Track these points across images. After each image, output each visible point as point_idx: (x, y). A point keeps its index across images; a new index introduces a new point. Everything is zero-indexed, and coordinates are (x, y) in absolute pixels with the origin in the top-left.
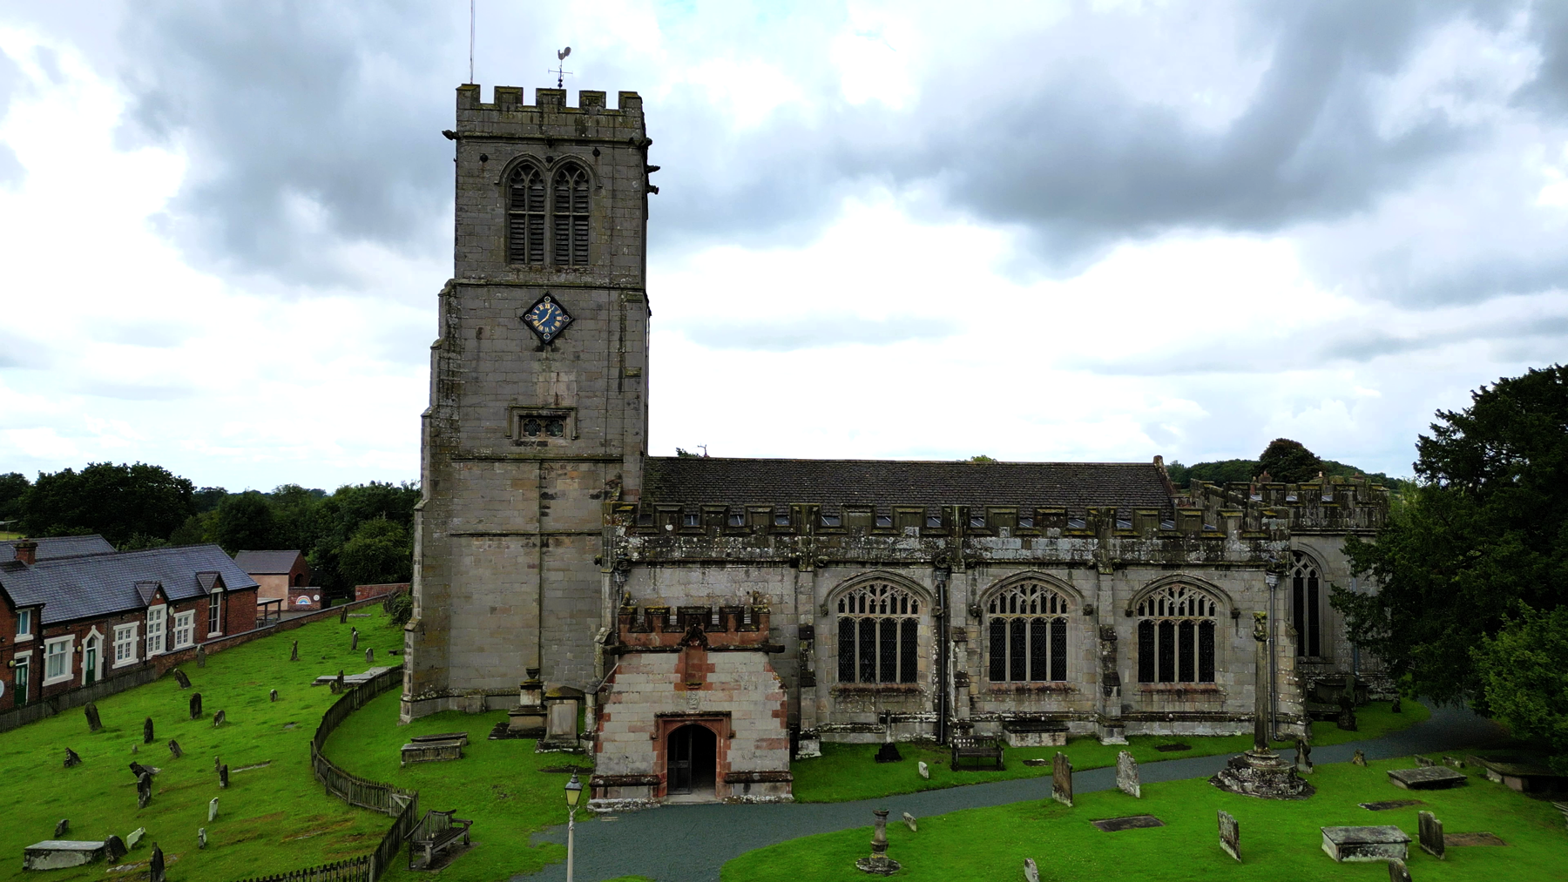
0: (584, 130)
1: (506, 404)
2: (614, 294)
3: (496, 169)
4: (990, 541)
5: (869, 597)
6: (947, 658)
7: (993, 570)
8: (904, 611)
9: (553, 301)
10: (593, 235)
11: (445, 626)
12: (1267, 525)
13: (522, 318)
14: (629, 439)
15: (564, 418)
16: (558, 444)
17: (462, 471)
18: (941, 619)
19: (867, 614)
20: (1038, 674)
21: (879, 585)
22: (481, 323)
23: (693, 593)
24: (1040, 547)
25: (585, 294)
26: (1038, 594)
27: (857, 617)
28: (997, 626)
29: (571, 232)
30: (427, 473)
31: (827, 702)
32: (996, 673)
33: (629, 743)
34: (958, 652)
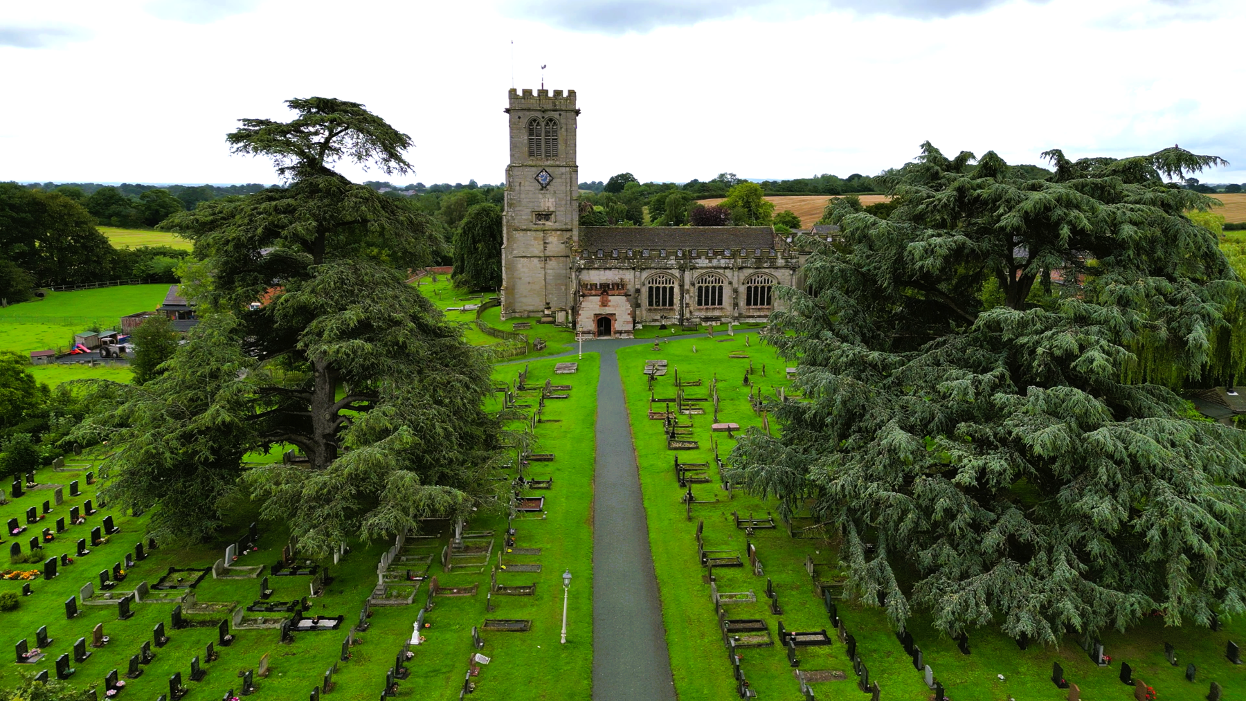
3: (524, 122)
11: (513, 289)
16: (548, 223)
17: (517, 235)
18: (682, 286)
20: (713, 303)
27: (654, 286)
28: (700, 289)
31: (644, 313)
32: (700, 303)
33: (586, 320)
34: (687, 296)
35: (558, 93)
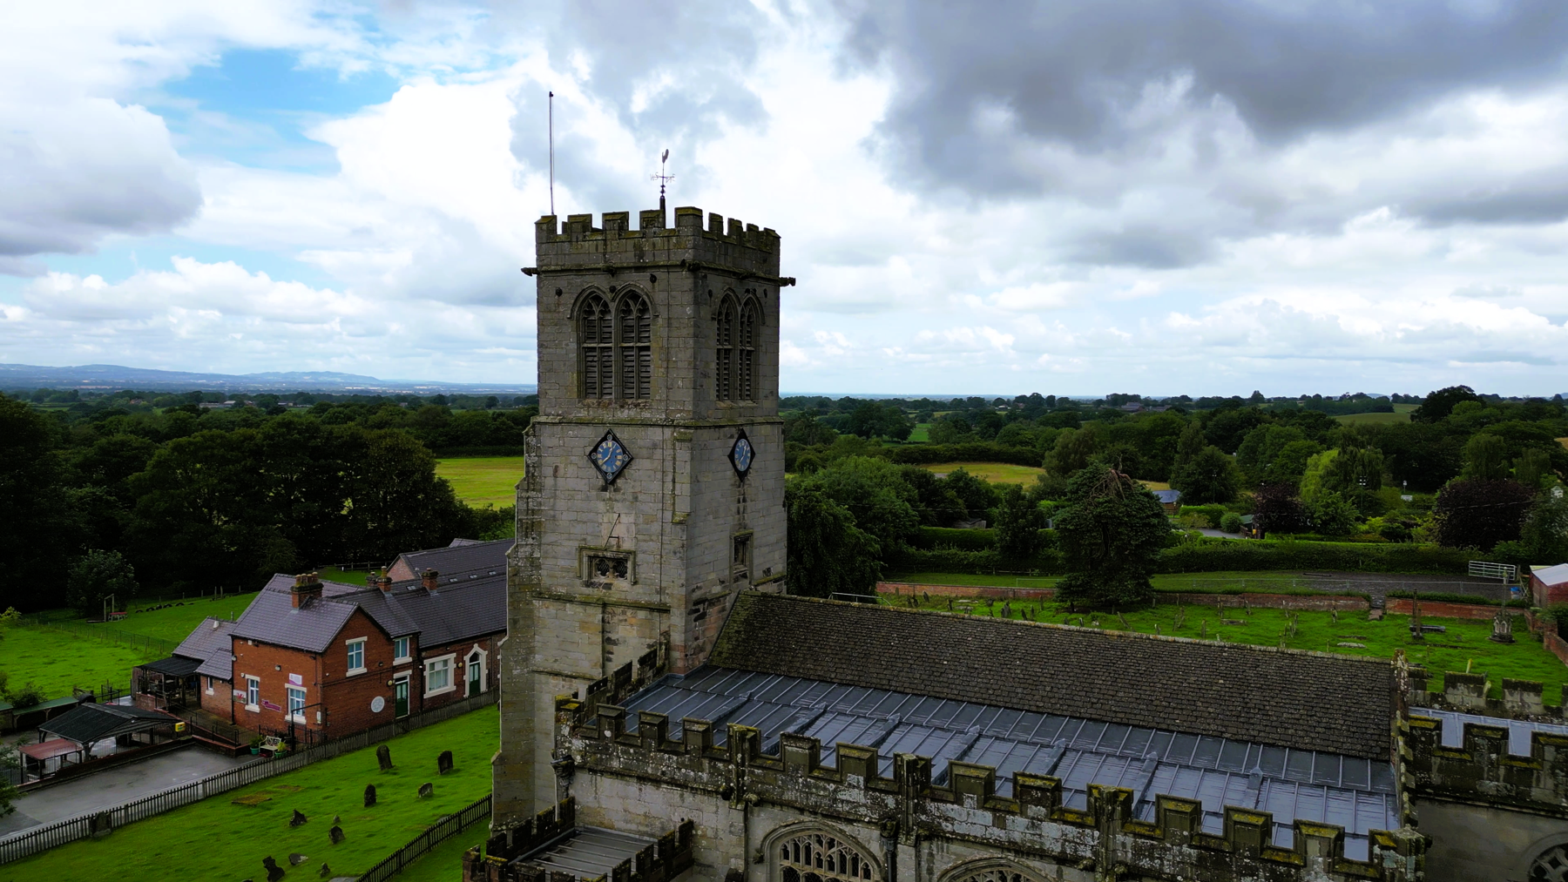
0: (641, 255)
1: (576, 544)
2: (668, 431)
4: (951, 809)
5: (815, 847)
7: (955, 848)
9: (615, 439)
12: (1381, 858)
16: (622, 587)
23: (632, 809)
24: (1018, 828)
25: (641, 432)
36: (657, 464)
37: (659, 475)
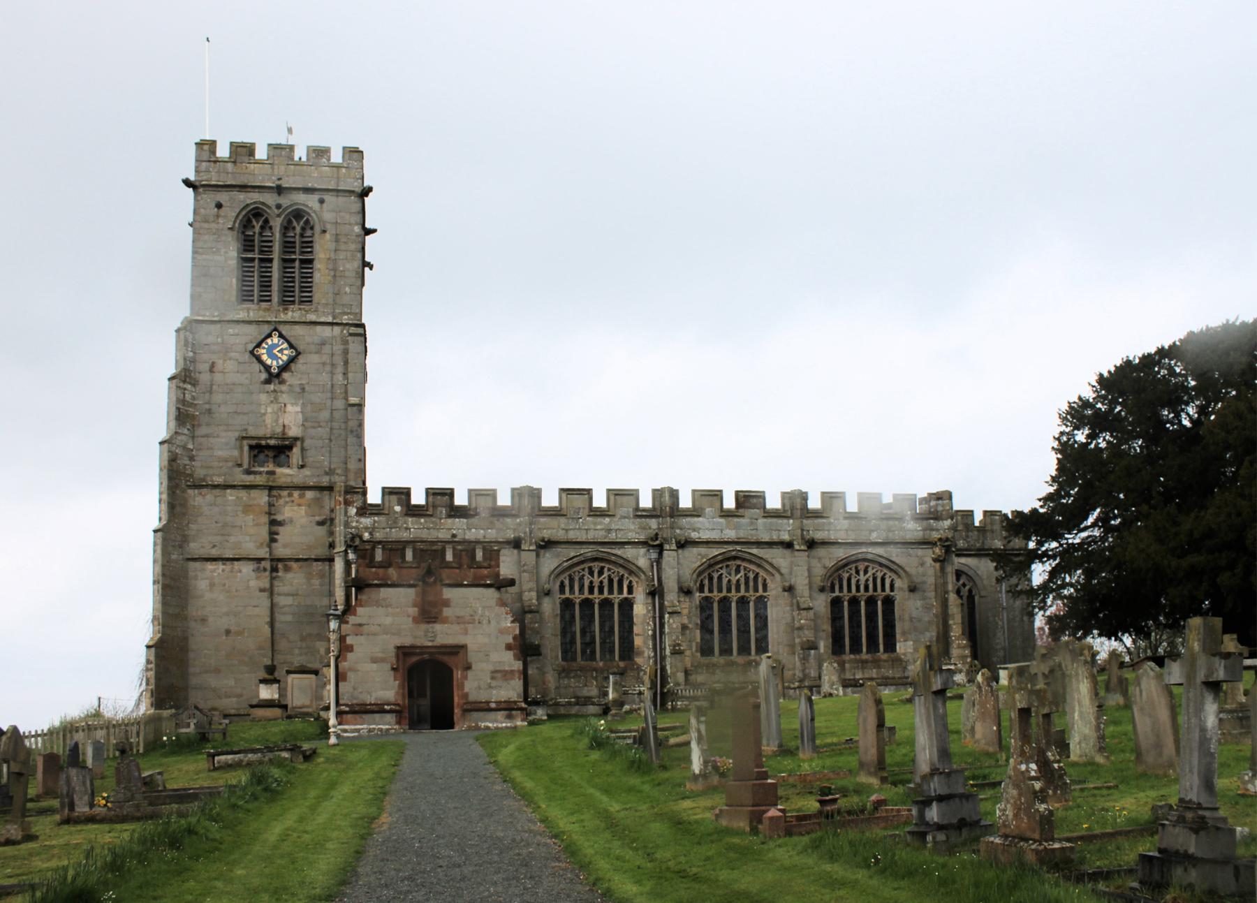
1: (237, 434)
2: (337, 329)
6: (662, 633)
8: (620, 591)
9: (281, 336)
10: (317, 276)
13: (252, 352)
14: (352, 465)
15: (290, 448)
16: (286, 474)
17: (199, 500)
18: (656, 593)
19: (586, 595)
21: (596, 566)
22: (214, 357)
26: (742, 573)
27: (577, 597)
28: (706, 605)
29: (297, 275)
30: (165, 496)
32: (706, 650)
34: (672, 624)
35: (320, 153)
36: (326, 358)
37: (328, 368)
